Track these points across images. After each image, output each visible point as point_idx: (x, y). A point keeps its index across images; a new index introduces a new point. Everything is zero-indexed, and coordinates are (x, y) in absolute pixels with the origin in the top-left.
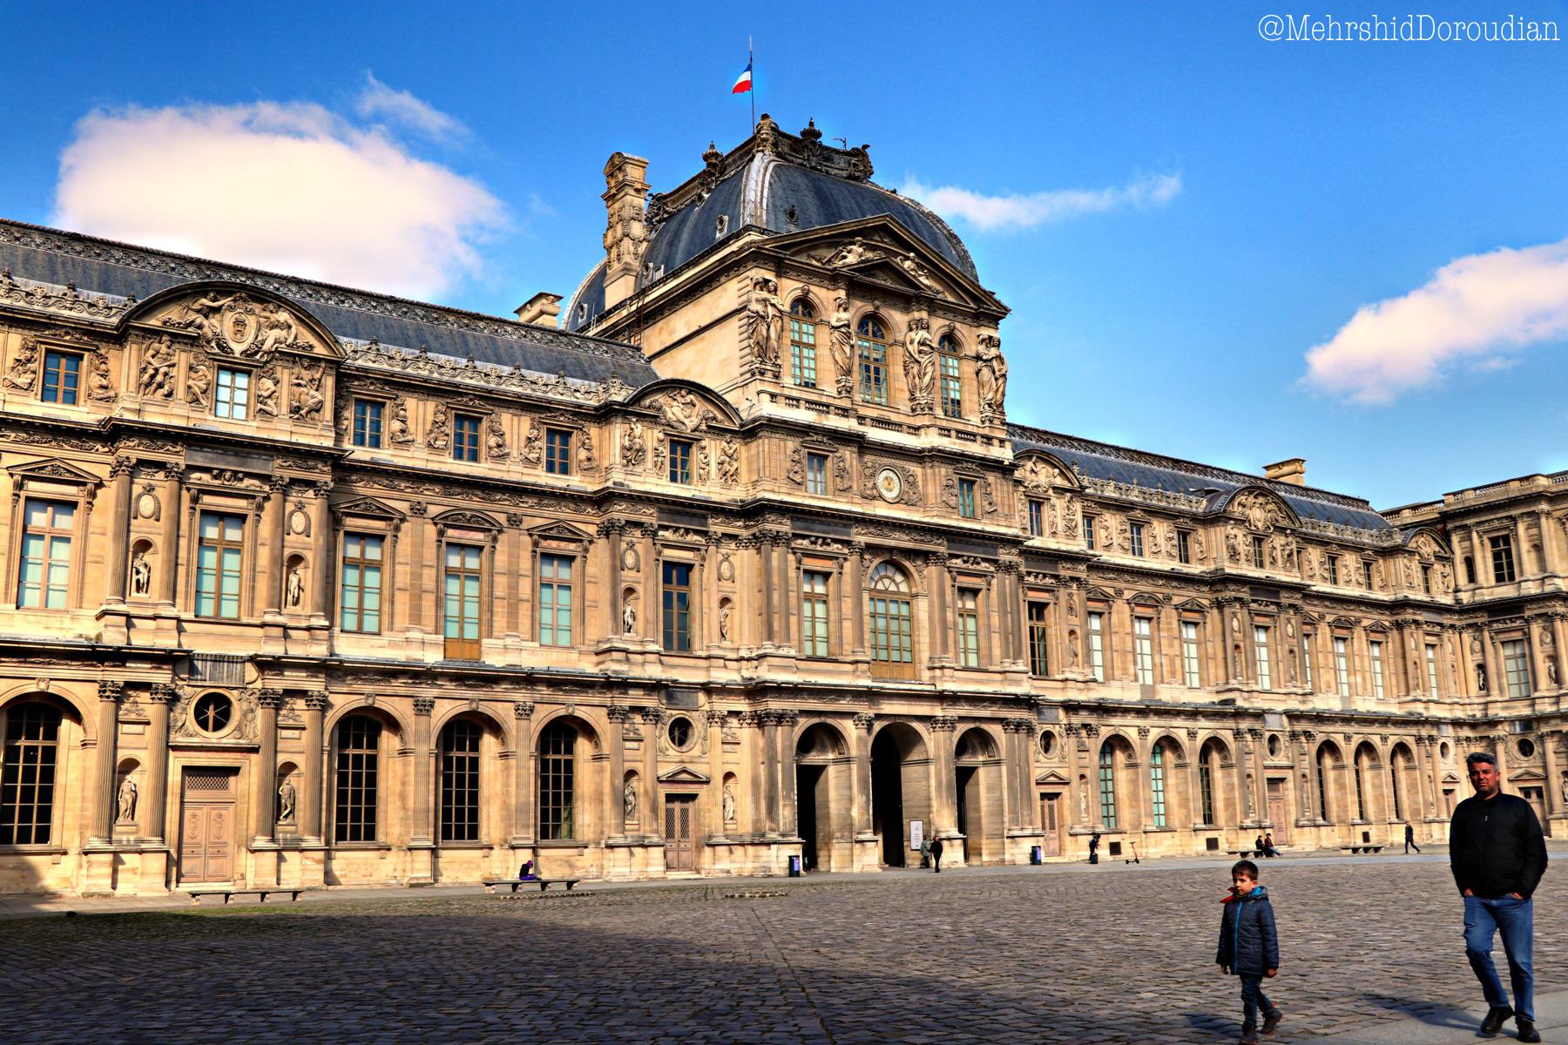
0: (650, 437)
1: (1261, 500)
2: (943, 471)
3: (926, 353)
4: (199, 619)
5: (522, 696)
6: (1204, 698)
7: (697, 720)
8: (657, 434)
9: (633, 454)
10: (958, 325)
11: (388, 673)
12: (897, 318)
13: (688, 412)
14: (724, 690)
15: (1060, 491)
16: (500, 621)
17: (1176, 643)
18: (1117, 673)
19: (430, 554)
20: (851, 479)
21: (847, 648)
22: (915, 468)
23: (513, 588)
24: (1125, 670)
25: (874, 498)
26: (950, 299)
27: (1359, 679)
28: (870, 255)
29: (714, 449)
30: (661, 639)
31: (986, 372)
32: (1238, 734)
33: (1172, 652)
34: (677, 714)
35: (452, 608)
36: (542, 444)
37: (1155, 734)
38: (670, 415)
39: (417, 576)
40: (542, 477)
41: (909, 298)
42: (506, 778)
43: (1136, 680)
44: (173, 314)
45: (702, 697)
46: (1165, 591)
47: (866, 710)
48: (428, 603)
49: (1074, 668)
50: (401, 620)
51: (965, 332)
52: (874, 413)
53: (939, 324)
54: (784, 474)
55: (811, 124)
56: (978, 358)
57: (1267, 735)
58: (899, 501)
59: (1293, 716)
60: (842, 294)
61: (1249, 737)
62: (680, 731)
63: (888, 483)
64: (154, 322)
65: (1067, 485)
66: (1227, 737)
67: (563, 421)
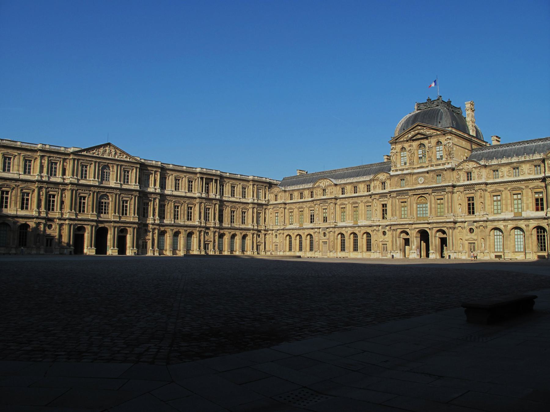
0: (377, 183)
5: (359, 229)
7: (386, 231)
9: (375, 187)
11: (342, 227)
12: (425, 142)
18: (504, 210)
22: (427, 175)
24: (507, 210)
28: (416, 132)
30: (381, 217)
33: (528, 202)
37: (510, 226)
41: (427, 137)
42: (362, 242)
46: (526, 185)
52: (419, 166)
62: (384, 233)
63: (421, 180)
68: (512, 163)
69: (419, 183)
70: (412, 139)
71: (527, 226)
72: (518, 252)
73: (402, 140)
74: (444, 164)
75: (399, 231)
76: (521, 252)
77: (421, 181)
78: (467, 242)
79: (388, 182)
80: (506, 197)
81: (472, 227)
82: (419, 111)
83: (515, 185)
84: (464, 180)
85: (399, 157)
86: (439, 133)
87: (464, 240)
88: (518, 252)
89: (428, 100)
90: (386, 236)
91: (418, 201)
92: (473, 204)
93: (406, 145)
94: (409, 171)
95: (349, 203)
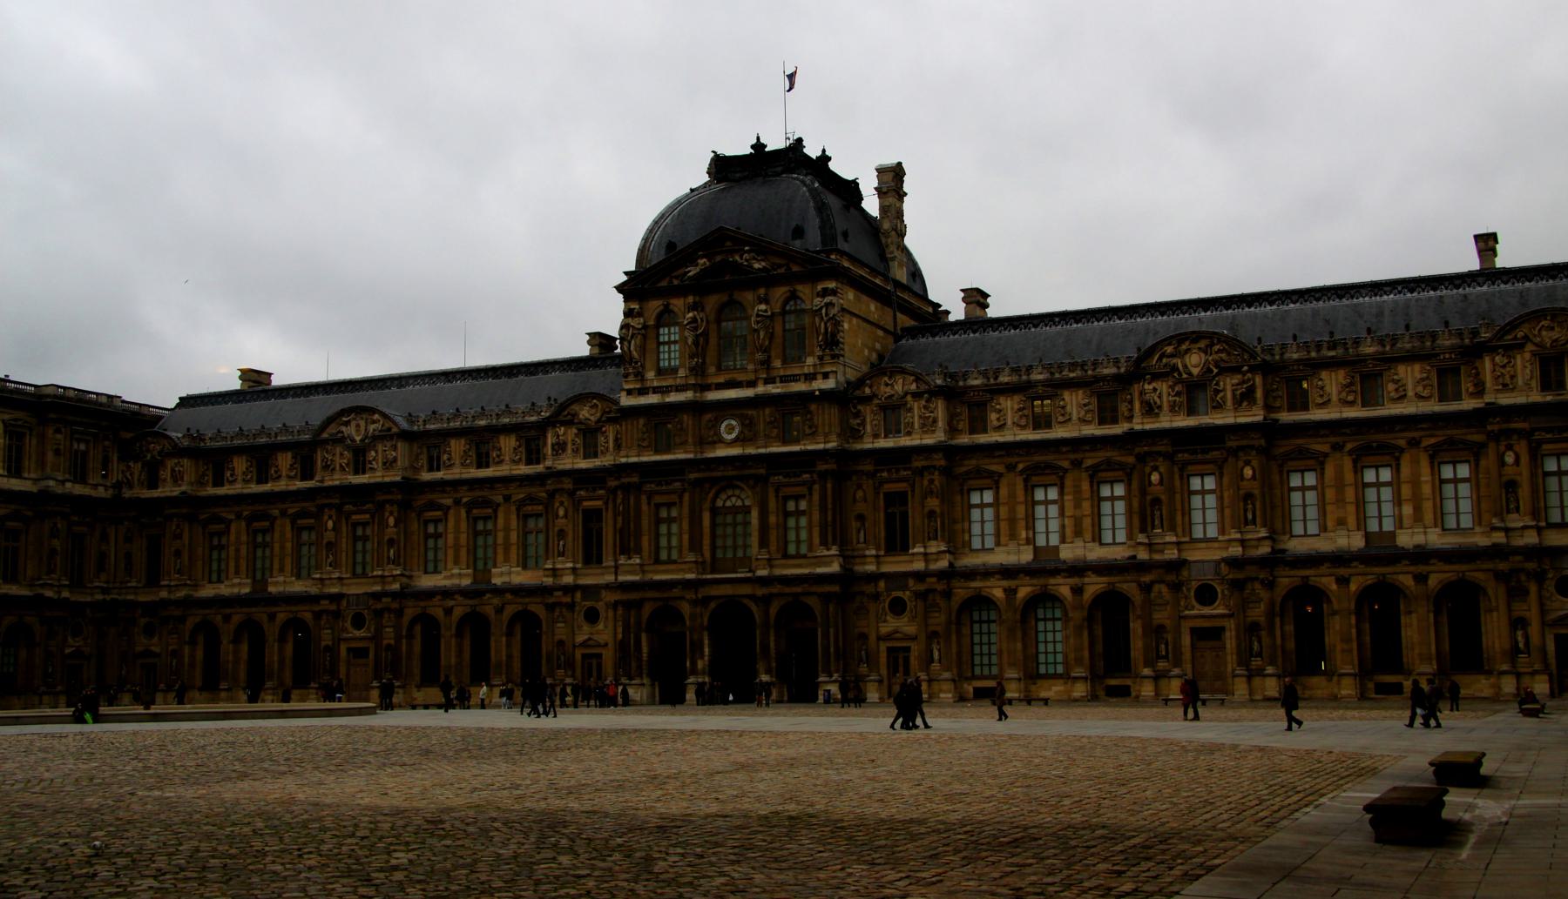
1: (1202, 344)
4: (354, 575)
5: (496, 601)
6: (1119, 553)
7: (600, 606)
8: (575, 431)
9: (560, 448)
10: (799, 287)
11: (429, 594)
14: (607, 587)
16: (500, 557)
17: (1086, 505)
18: (1003, 539)
19: (464, 526)
21: (685, 551)
23: (507, 538)
24: (1013, 536)
26: (795, 268)
27: (1407, 510)
32: (1146, 588)
34: (589, 604)
35: (480, 553)
36: (523, 449)
37: (1023, 592)
39: (457, 539)
40: (524, 470)
43: (1030, 541)
44: (332, 429)
45: (604, 593)
47: (690, 595)
48: (463, 552)
49: (933, 543)
50: (450, 565)
52: (721, 380)
53: (780, 292)
57: (1194, 584)
59: (1233, 563)
61: (1164, 589)
62: (592, 616)
64: (325, 435)
65: (924, 387)
66: (1129, 587)
67: (533, 433)
68: (1030, 385)
70: (699, 287)
71: (1077, 591)
72: (1047, 676)
73: (664, 283)
74: (810, 377)
75: (647, 610)
76: (1055, 676)
78: (883, 646)
79: (611, 431)
80: (1012, 495)
81: (899, 594)
82: (722, 186)
83: (1037, 458)
84: (876, 436)
85: (651, 345)
86: (795, 268)
87: (873, 637)
88: (1047, 676)
90: (601, 626)
91: (719, 503)
92: (905, 516)
93: (678, 304)
94: (688, 395)
95: (457, 502)
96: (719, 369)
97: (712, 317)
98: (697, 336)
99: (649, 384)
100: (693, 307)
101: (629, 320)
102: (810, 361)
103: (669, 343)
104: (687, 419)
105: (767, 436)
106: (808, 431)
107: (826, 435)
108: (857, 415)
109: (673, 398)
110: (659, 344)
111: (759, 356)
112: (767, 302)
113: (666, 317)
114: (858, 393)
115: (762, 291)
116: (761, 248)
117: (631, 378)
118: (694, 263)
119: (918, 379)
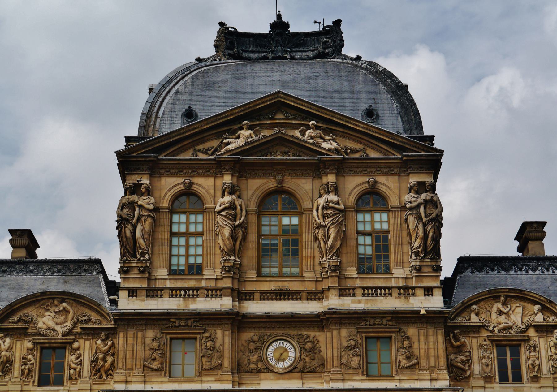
2: (344, 332)
3: (328, 216)
10: (381, 179)
12: (303, 186)
13: (61, 318)
15: (540, 329)
20: (221, 357)
25: (259, 371)
26: (373, 154)
28: (266, 133)
29: (87, 348)
31: (411, 219)
38: (40, 325)
51: (388, 184)
52: (267, 286)
53: (354, 184)
54: (139, 363)
55: (279, 16)
56: (403, 208)
58: (291, 371)
60: (227, 179)
69: (268, 369)
73: (187, 155)
74: (407, 291)
77: (279, 360)
86: (373, 154)
89: (272, 26)
93: (205, 184)
94: (225, 303)
96: (259, 274)
97: (253, 206)
98: (234, 228)
99: (159, 284)
100: (232, 190)
101: (135, 198)
102: (397, 271)
103: (187, 234)
104: (222, 337)
105: (346, 366)
106: (404, 363)
107: (432, 370)
108: (460, 349)
109: (202, 304)
110: (173, 234)
111: (329, 261)
112: (336, 191)
113: (188, 200)
114: (460, 320)
115: (331, 179)
116: (330, 124)
117: (134, 273)
118: (234, 133)
119: (544, 309)
